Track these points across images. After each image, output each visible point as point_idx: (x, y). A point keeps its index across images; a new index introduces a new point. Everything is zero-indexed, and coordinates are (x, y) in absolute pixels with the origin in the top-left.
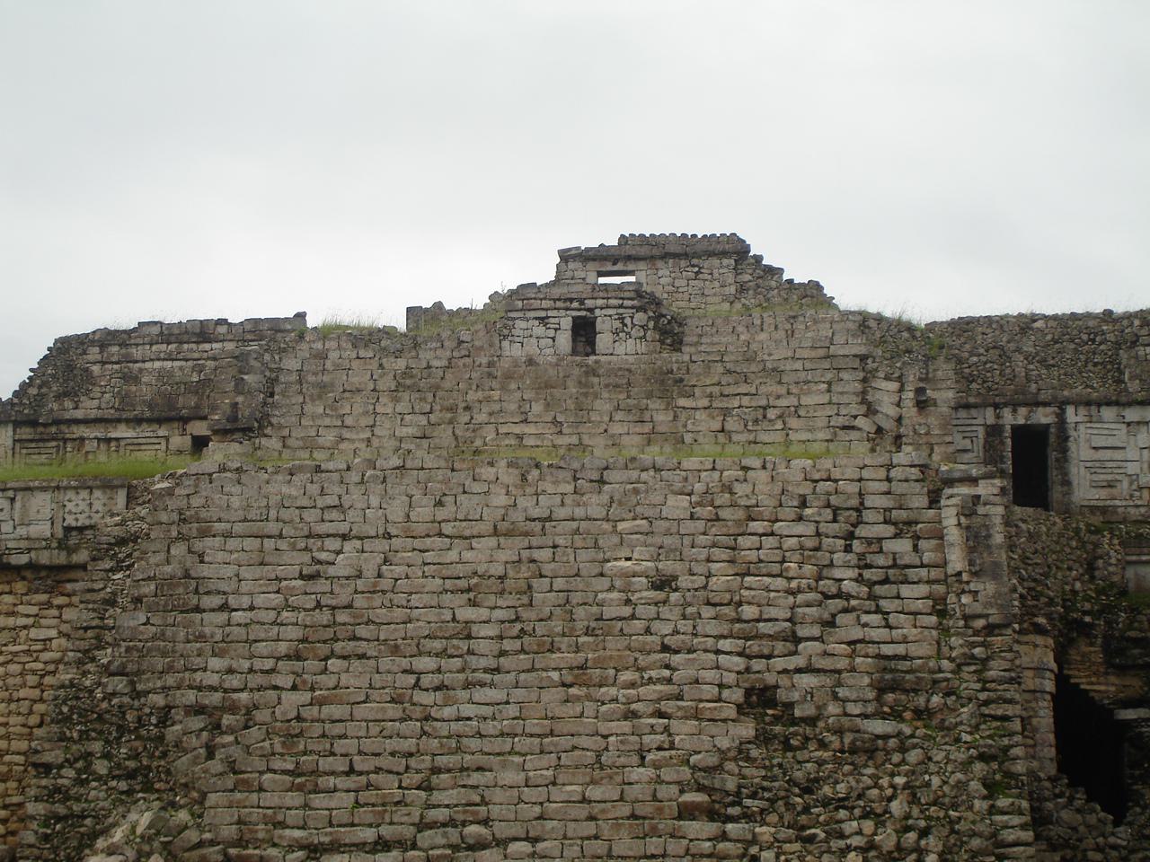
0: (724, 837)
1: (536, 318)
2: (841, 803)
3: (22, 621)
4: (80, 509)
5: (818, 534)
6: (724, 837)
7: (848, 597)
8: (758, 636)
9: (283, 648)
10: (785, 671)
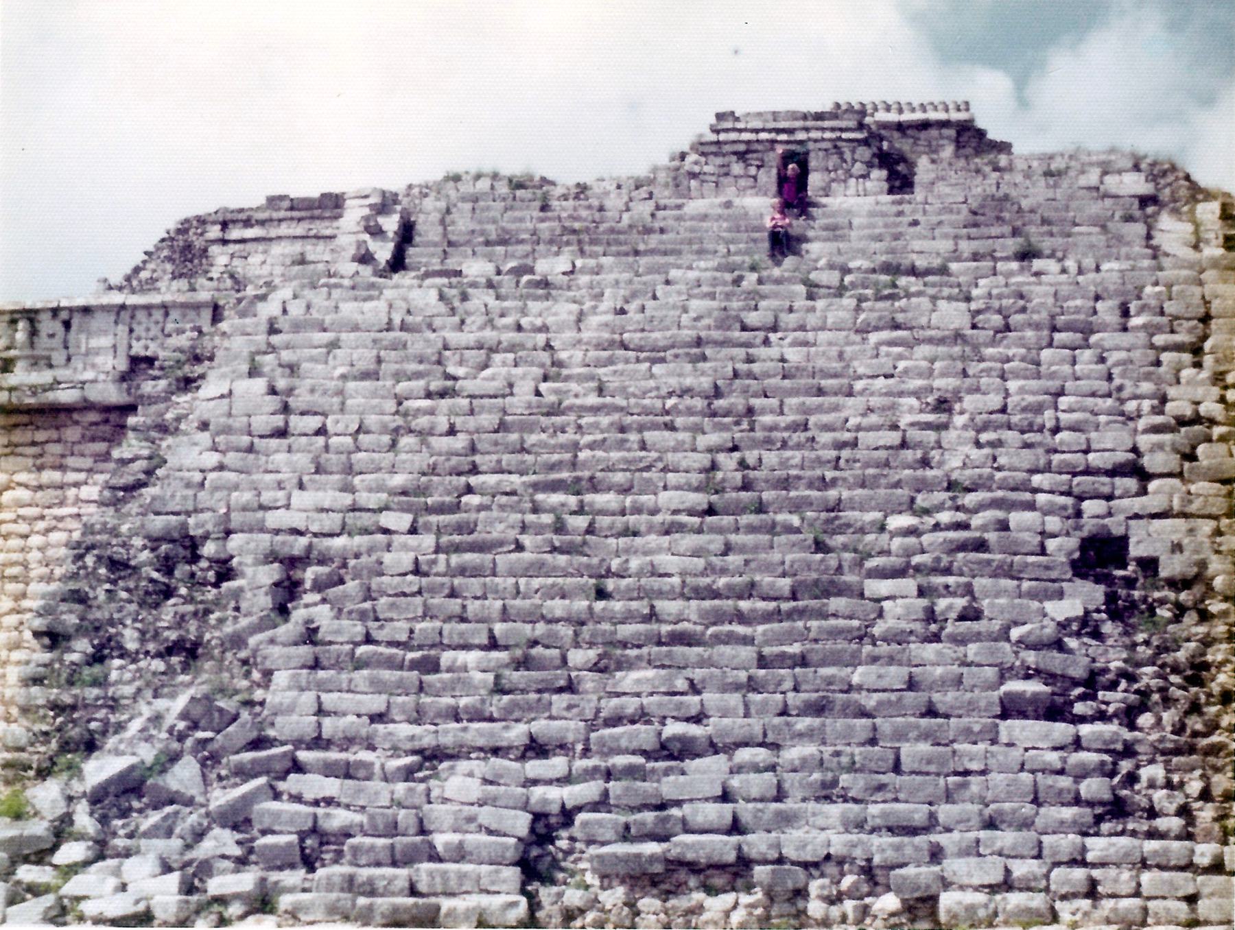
0: (1078, 744)
1: (735, 153)
3: (72, 477)
4: (151, 334)
5: (1152, 346)
6: (1078, 744)
7: (1212, 422)
8: (1088, 472)
9: (398, 480)
10: (1137, 516)
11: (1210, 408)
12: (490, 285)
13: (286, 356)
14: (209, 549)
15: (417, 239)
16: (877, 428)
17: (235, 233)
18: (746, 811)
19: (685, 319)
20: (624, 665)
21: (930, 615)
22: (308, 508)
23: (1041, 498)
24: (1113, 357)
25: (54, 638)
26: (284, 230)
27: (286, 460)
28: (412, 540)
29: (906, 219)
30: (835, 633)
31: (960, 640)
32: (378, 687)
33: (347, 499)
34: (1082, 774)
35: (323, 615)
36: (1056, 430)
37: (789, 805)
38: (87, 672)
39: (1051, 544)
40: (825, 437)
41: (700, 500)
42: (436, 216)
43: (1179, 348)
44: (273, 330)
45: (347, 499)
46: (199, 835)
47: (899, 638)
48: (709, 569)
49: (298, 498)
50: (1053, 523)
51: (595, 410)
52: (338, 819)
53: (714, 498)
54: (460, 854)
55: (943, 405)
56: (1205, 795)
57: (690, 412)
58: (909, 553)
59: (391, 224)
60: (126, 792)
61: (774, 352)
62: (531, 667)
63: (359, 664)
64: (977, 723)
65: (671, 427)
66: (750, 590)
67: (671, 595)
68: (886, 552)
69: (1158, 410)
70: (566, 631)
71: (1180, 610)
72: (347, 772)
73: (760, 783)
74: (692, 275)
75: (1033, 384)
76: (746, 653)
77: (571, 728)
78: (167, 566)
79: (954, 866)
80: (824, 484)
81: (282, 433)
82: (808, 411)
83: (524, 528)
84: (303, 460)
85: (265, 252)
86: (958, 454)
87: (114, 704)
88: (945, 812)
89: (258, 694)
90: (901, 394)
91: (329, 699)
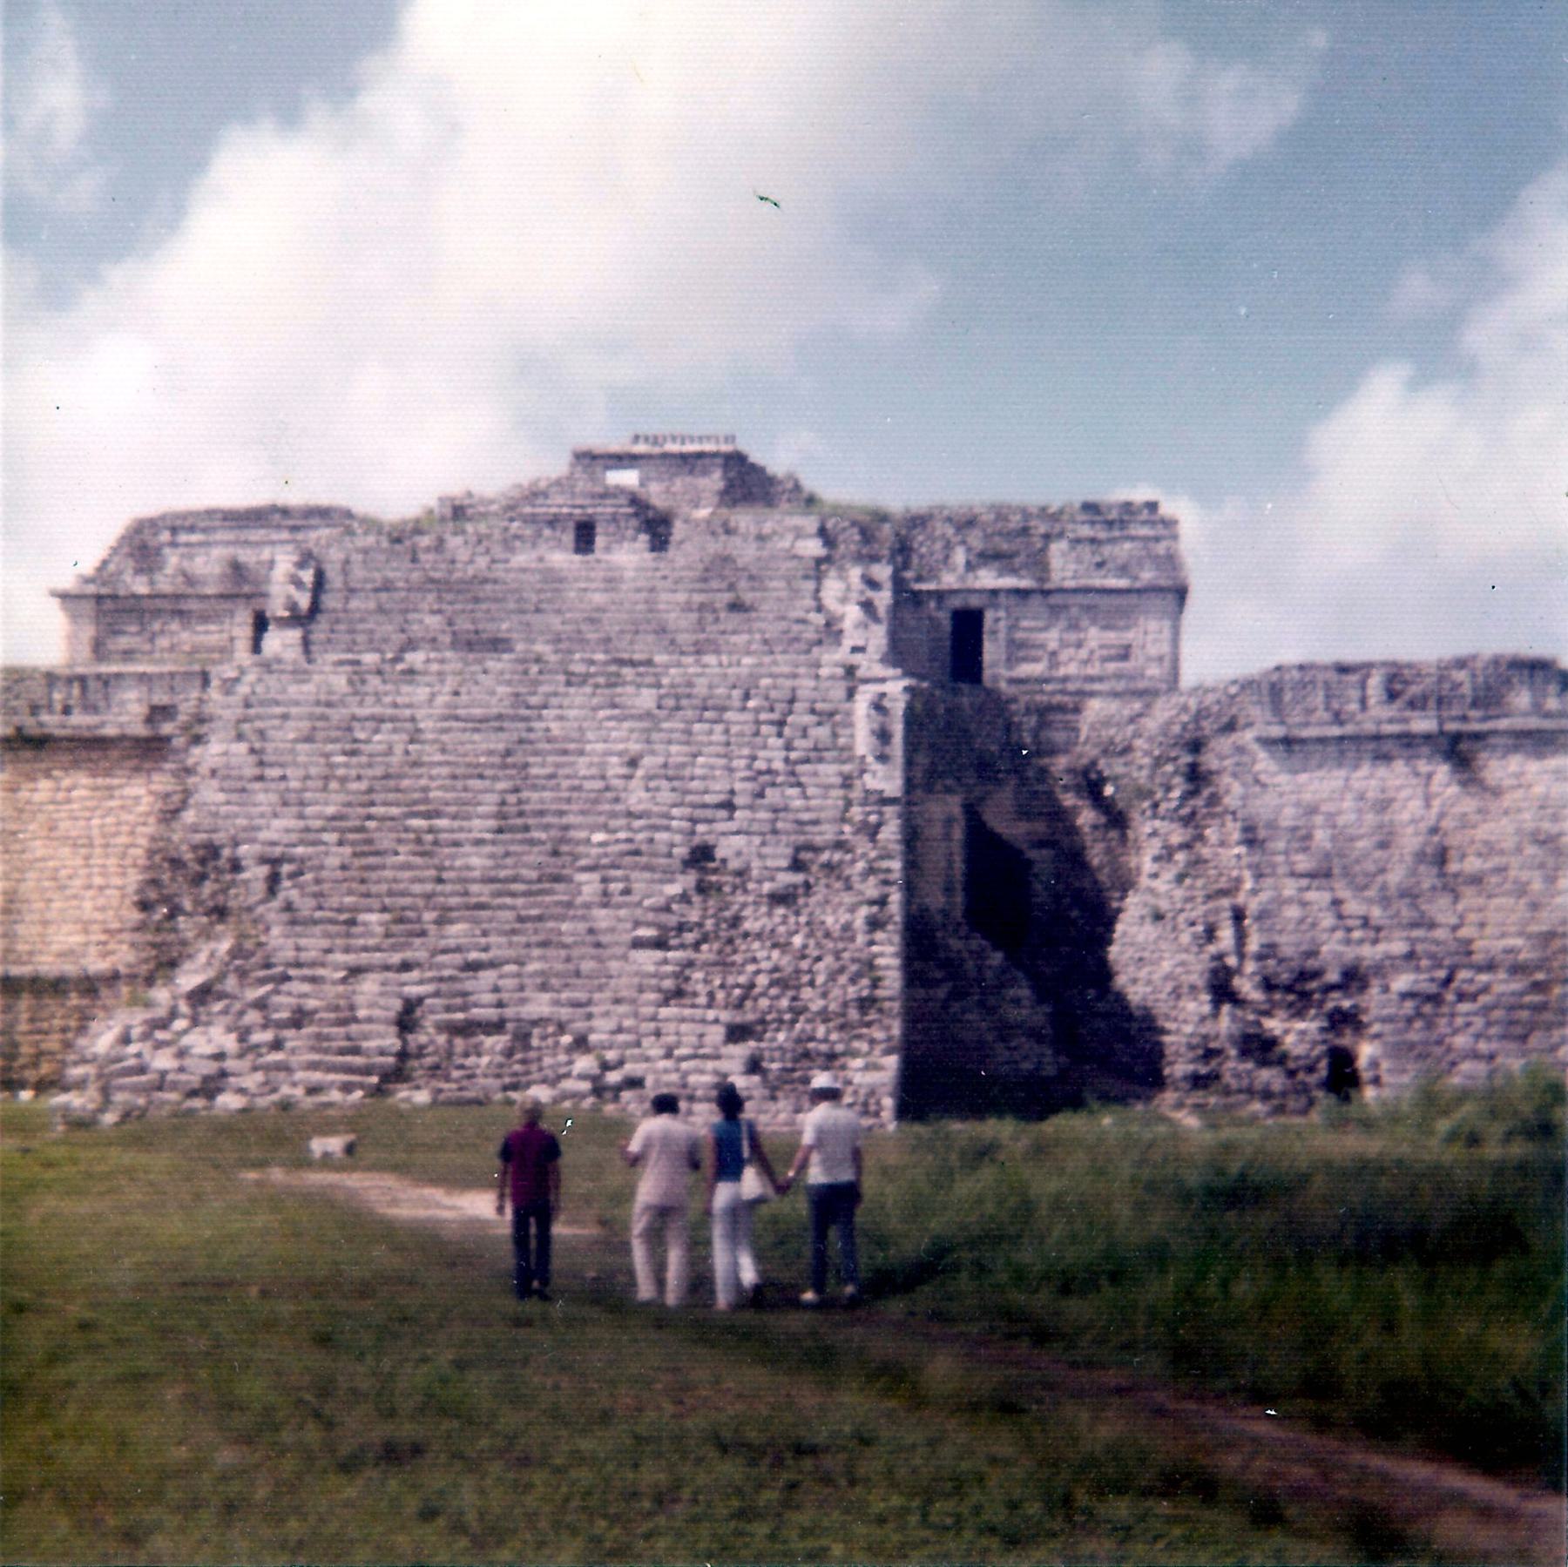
2: (759, 936)
6: (665, 962)
8: (705, 806)
9: (330, 810)
10: (724, 834)
11: (778, 765)
12: (379, 672)
13: (259, 724)
14: (226, 852)
15: (327, 587)
16: (593, 777)
17: (183, 538)
18: (505, 996)
19: (494, 701)
20: (451, 922)
21: (605, 893)
22: (278, 829)
23: (674, 823)
24: (734, 729)
25: (144, 906)
26: (219, 536)
27: (264, 798)
28: (341, 850)
29: (658, 574)
30: (558, 903)
31: (619, 906)
32: (328, 935)
33: (301, 824)
34: (662, 977)
35: (294, 894)
36: (692, 778)
37: (527, 994)
38: (167, 925)
39: (676, 851)
40: (565, 783)
41: (492, 823)
42: (338, 566)
43: (772, 723)
44: (247, 705)
45: (301, 824)
46: (241, 1013)
47: (587, 906)
48: (498, 867)
49: (276, 823)
50: (678, 838)
51: (440, 764)
52: (311, 1003)
53: (502, 823)
54: (370, 1020)
55: (633, 763)
56: (722, 986)
57: (492, 766)
58: (599, 857)
59: (308, 576)
60: (201, 995)
61: (542, 725)
62: (404, 925)
63: (315, 922)
64: (619, 951)
65: (481, 777)
66: (515, 879)
67: (474, 881)
68: (587, 856)
69: (749, 767)
70: (421, 902)
71: (735, 888)
72: (313, 980)
73: (508, 983)
74: (499, 666)
75: (685, 749)
76: (509, 915)
77: (421, 955)
78: (202, 861)
79: (597, 1023)
80: (561, 813)
81: (261, 778)
82: (558, 765)
83: (400, 841)
84: (273, 798)
85: (207, 554)
86: (636, 797)
87: (184, 943)
88: (597, 996)
89: (263, 939)
90: (611, 754)
91: (303, 942)
